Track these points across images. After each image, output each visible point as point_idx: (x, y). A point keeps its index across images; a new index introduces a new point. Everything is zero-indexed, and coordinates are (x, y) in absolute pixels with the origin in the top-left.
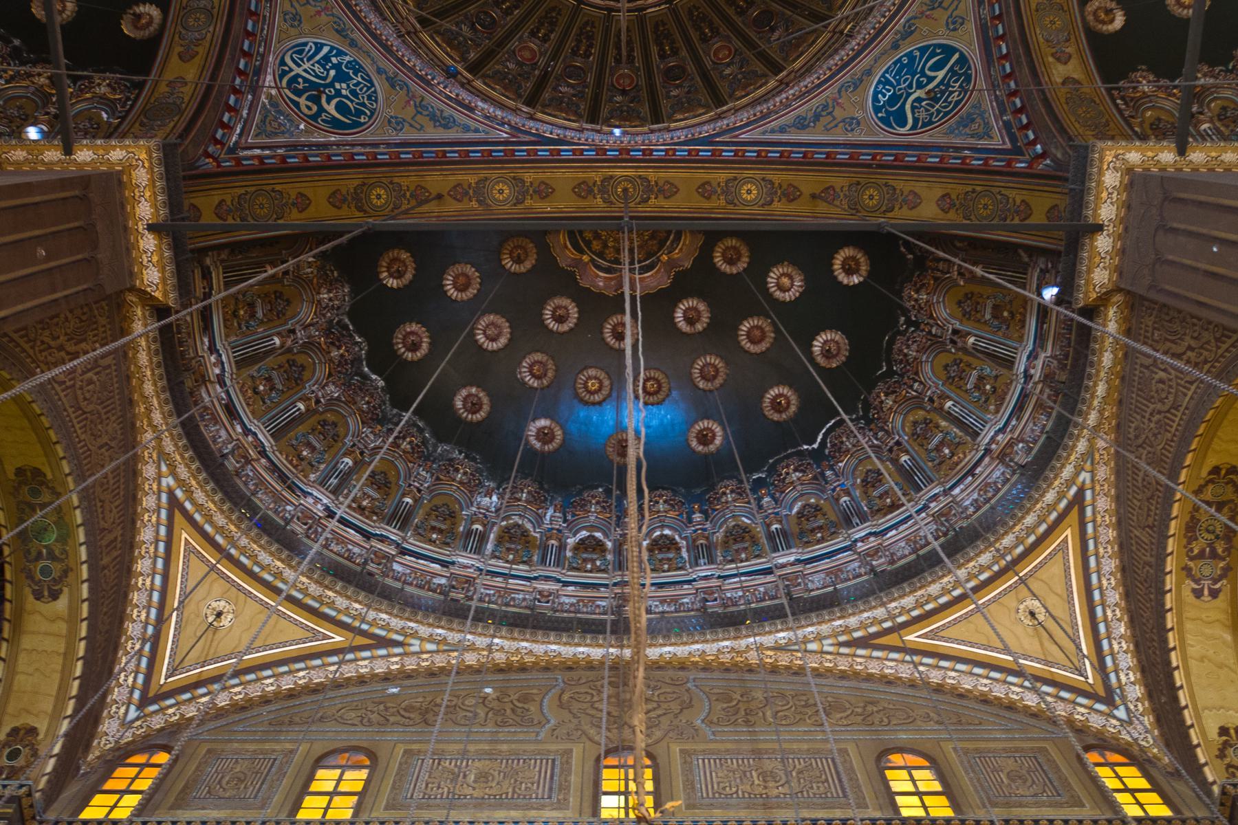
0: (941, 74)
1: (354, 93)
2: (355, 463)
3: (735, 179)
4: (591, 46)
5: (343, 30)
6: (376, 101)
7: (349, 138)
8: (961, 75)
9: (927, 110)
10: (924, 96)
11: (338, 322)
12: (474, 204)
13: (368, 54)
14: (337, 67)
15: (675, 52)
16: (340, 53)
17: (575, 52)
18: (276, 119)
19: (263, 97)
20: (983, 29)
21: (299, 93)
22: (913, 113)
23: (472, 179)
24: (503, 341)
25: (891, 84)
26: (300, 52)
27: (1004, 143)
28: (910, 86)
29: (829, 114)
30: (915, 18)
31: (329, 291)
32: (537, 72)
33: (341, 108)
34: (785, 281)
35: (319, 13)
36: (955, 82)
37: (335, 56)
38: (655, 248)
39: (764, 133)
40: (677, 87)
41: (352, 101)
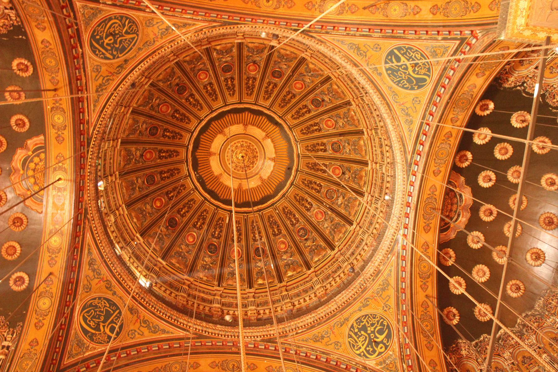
0: (403, 59)
1: (372, 325)
2: (545, 352)
4: (315, 183)
5: (341, 323)
6: (376, 315)
7: (395, 332)
8: (407, 51)
9: (421, 69)
11: (475, 347)
12: (429, 280)
13: (351, 314)
14: (360, 330)
15: (323, 144)
16: (352, 326)
17: (319, 192)
18: (387, 365)
19: (377, 368)
21: (374, 351)
22: (420, 75)
23: (418, 280)
24: (486, 269)
25: (401, 80)
26: (354, 346)
27: (455, 43)
28: (405, 73)
29: (407, 109)
31: (462, 350)
32: (329, 213)
33: (381, 332)
35: (333, 333)
36: (410, 54)
37: (354, 329)
38: (453, 193)
40: (344, 147)
41: (376, 327)
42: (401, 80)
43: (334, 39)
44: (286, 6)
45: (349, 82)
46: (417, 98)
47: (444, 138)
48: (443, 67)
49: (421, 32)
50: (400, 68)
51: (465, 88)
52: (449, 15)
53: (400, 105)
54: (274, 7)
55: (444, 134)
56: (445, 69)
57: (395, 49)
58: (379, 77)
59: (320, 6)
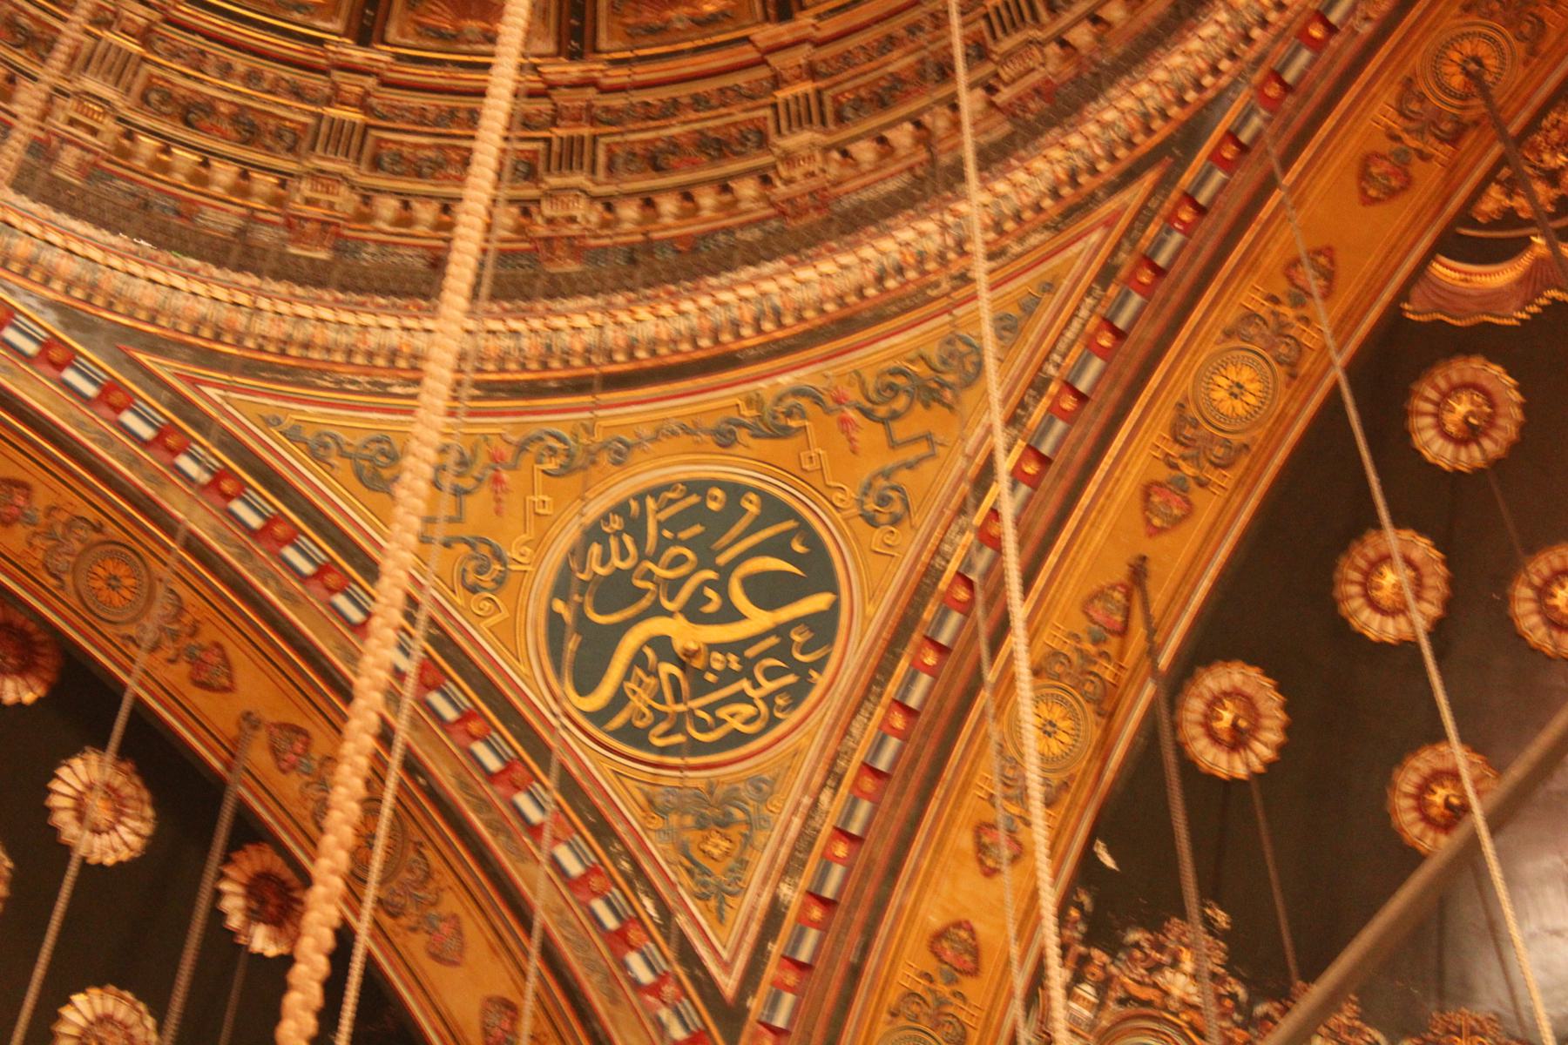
0: (758, 620)
3: (98, 528)
10: (678, 645)
20: (923, 584)
22: (627, 676)
25: (640, 541)
28: (673, 587)
30: (817, 400)
34: (99, 810)
36: (771, 674)
39: (269, 422)
42: (640, 541)
43: (1049, 287)
44: (1387, 146)
45: (710, 122)
46: (500, 582)
47: (204, 639)
48: (620, 828)
49: (864, 807)
51: (452, 903)
52: (902, 1022)
53: (496, 459)
54: (1421, 86)
55: (234, 654)
56: (603, 831)
57: (835, 607)
58: (710, 423)
59: (1281, 329)
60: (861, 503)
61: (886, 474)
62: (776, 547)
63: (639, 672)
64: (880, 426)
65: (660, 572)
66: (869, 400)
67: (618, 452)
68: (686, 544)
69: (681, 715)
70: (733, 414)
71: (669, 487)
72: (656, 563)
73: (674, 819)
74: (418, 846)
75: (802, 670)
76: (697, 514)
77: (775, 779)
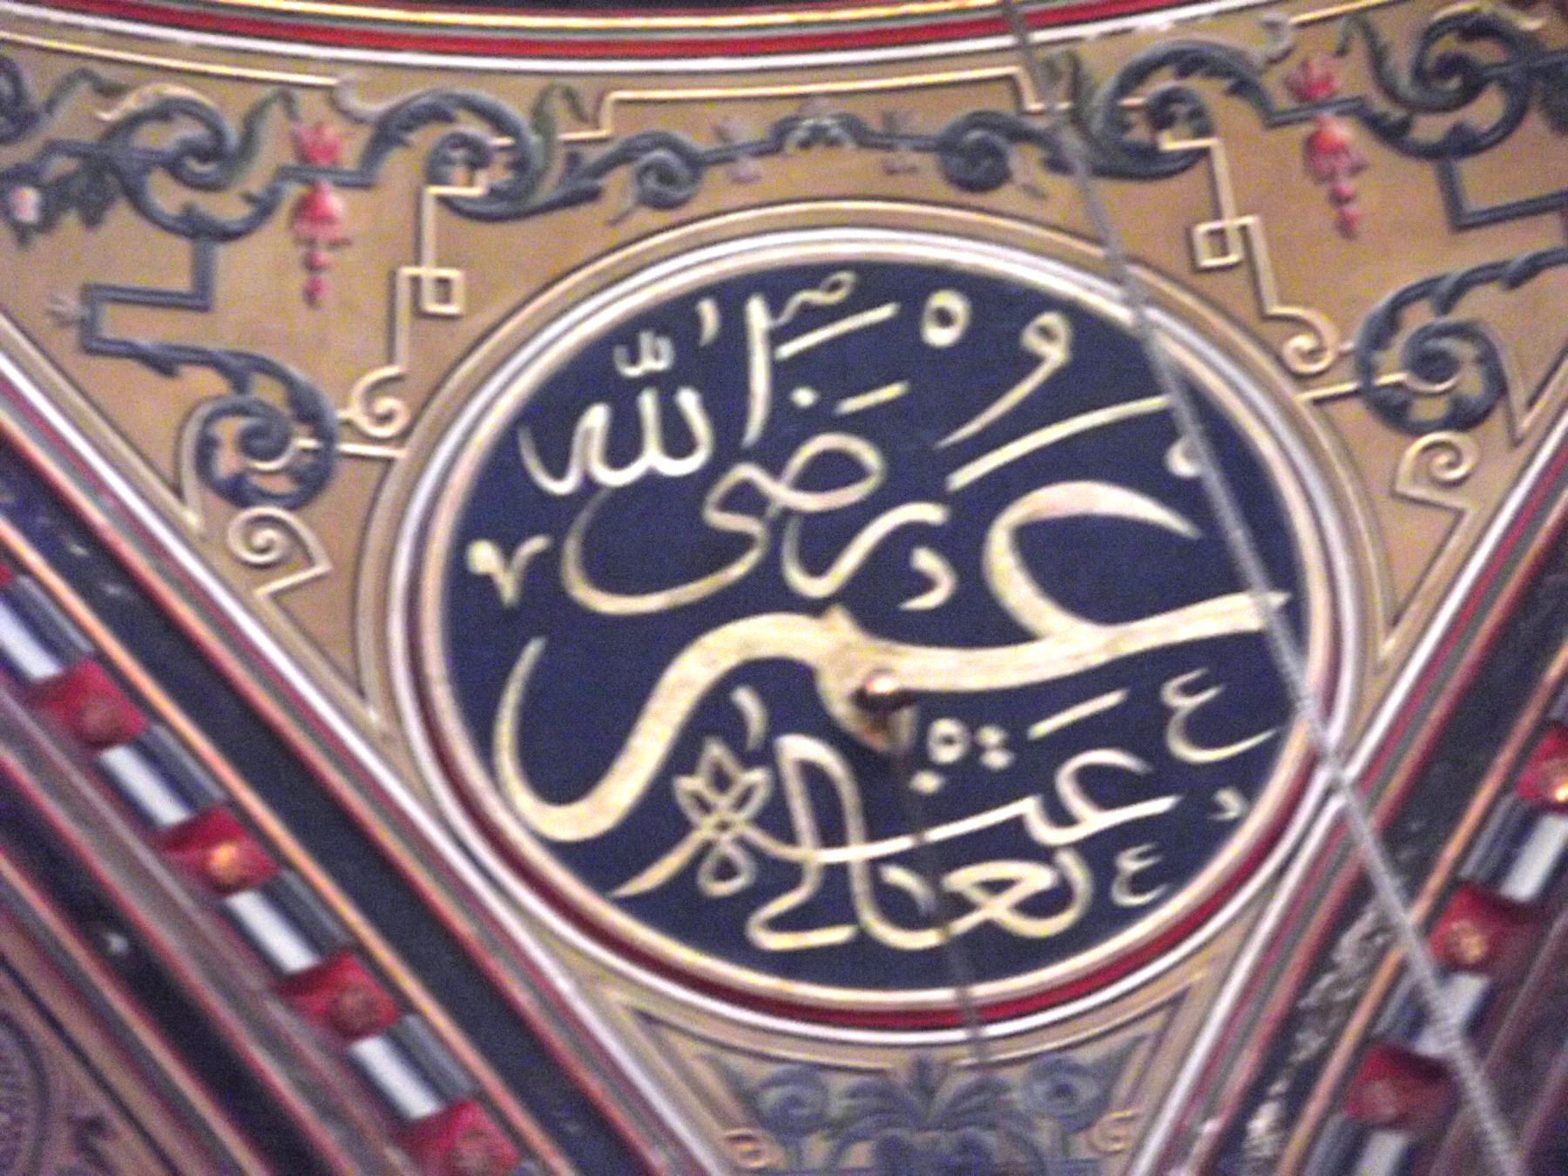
0: (1065, 643)
22: (682, 757)
25: (727, 407)
28: (822, 539)
30: (1244, 86)
36: (1103, 787)
42: (727, 407)
46: (311, 482)
50: (930, 513)
53: (309, 161)
58: (933, 121)
60: (1367, 370)
61: (1447, 294)
62: (1130, 456)
63: (715, 751)
64: (1424, 174)
65: (782, 493)
66: (1391, 92)
67: (666, 176)
68: (857, 424)
69: (836, 875)
70: (999, 103)
71: (814, 274)
72: (775, 470)
73: (817, 1149)
74: (89, 1131)
75: (1198, 787)
76: (893, 350)
77: (1110, 1069)
